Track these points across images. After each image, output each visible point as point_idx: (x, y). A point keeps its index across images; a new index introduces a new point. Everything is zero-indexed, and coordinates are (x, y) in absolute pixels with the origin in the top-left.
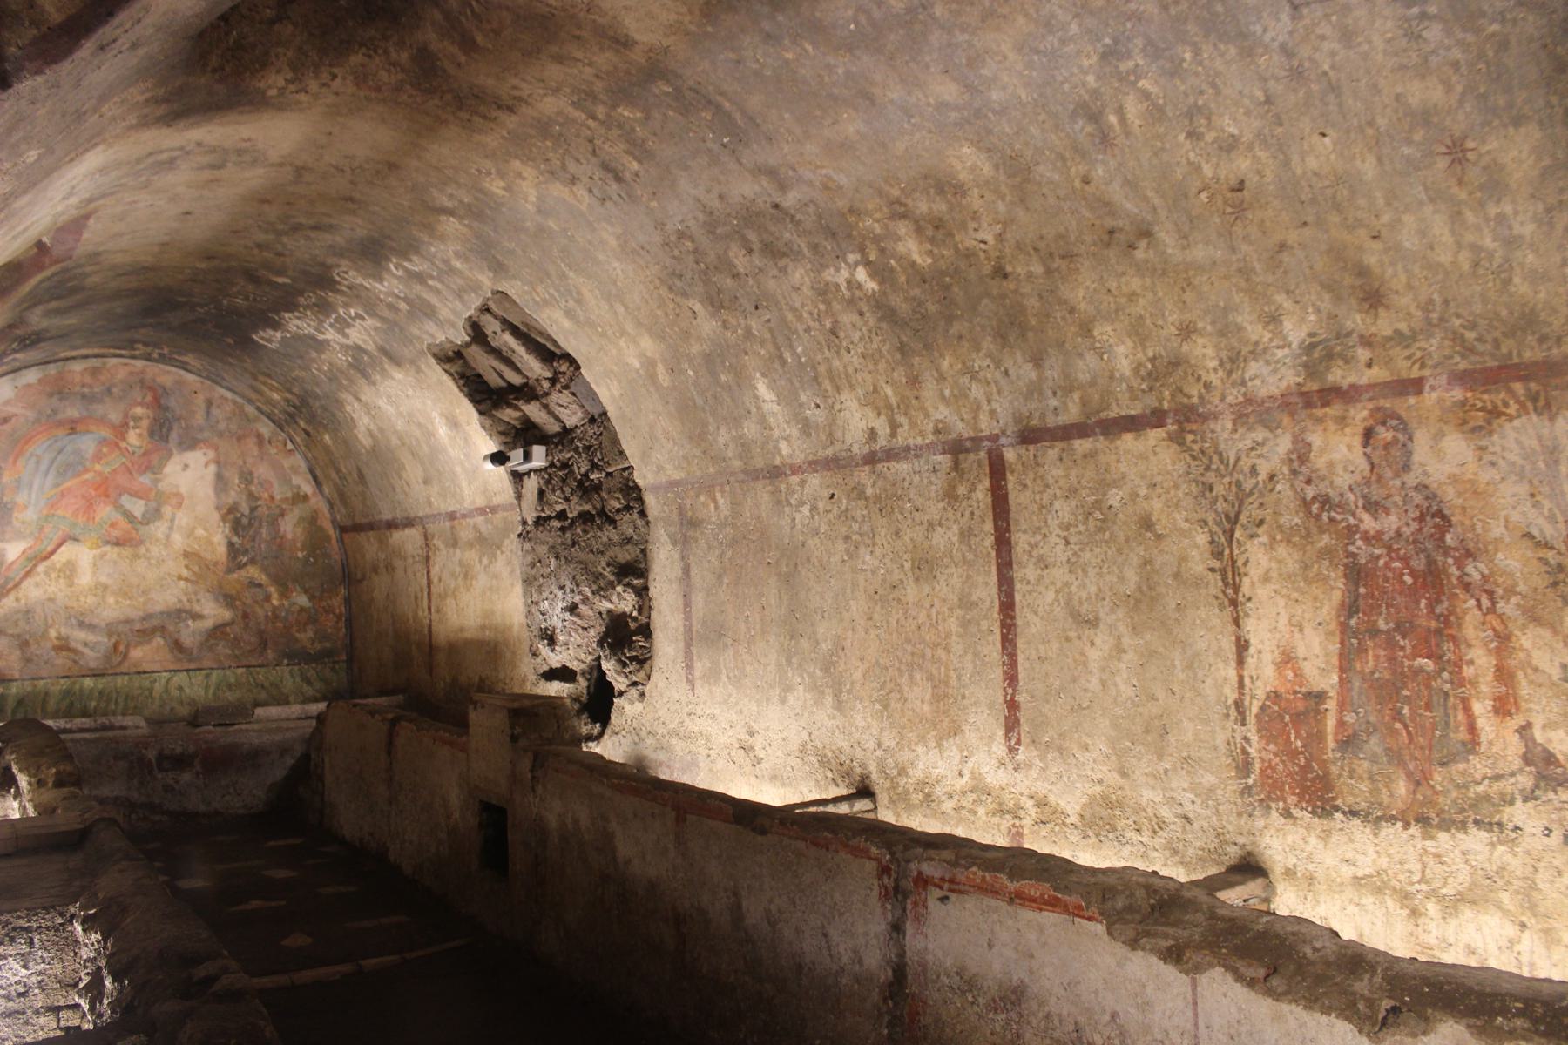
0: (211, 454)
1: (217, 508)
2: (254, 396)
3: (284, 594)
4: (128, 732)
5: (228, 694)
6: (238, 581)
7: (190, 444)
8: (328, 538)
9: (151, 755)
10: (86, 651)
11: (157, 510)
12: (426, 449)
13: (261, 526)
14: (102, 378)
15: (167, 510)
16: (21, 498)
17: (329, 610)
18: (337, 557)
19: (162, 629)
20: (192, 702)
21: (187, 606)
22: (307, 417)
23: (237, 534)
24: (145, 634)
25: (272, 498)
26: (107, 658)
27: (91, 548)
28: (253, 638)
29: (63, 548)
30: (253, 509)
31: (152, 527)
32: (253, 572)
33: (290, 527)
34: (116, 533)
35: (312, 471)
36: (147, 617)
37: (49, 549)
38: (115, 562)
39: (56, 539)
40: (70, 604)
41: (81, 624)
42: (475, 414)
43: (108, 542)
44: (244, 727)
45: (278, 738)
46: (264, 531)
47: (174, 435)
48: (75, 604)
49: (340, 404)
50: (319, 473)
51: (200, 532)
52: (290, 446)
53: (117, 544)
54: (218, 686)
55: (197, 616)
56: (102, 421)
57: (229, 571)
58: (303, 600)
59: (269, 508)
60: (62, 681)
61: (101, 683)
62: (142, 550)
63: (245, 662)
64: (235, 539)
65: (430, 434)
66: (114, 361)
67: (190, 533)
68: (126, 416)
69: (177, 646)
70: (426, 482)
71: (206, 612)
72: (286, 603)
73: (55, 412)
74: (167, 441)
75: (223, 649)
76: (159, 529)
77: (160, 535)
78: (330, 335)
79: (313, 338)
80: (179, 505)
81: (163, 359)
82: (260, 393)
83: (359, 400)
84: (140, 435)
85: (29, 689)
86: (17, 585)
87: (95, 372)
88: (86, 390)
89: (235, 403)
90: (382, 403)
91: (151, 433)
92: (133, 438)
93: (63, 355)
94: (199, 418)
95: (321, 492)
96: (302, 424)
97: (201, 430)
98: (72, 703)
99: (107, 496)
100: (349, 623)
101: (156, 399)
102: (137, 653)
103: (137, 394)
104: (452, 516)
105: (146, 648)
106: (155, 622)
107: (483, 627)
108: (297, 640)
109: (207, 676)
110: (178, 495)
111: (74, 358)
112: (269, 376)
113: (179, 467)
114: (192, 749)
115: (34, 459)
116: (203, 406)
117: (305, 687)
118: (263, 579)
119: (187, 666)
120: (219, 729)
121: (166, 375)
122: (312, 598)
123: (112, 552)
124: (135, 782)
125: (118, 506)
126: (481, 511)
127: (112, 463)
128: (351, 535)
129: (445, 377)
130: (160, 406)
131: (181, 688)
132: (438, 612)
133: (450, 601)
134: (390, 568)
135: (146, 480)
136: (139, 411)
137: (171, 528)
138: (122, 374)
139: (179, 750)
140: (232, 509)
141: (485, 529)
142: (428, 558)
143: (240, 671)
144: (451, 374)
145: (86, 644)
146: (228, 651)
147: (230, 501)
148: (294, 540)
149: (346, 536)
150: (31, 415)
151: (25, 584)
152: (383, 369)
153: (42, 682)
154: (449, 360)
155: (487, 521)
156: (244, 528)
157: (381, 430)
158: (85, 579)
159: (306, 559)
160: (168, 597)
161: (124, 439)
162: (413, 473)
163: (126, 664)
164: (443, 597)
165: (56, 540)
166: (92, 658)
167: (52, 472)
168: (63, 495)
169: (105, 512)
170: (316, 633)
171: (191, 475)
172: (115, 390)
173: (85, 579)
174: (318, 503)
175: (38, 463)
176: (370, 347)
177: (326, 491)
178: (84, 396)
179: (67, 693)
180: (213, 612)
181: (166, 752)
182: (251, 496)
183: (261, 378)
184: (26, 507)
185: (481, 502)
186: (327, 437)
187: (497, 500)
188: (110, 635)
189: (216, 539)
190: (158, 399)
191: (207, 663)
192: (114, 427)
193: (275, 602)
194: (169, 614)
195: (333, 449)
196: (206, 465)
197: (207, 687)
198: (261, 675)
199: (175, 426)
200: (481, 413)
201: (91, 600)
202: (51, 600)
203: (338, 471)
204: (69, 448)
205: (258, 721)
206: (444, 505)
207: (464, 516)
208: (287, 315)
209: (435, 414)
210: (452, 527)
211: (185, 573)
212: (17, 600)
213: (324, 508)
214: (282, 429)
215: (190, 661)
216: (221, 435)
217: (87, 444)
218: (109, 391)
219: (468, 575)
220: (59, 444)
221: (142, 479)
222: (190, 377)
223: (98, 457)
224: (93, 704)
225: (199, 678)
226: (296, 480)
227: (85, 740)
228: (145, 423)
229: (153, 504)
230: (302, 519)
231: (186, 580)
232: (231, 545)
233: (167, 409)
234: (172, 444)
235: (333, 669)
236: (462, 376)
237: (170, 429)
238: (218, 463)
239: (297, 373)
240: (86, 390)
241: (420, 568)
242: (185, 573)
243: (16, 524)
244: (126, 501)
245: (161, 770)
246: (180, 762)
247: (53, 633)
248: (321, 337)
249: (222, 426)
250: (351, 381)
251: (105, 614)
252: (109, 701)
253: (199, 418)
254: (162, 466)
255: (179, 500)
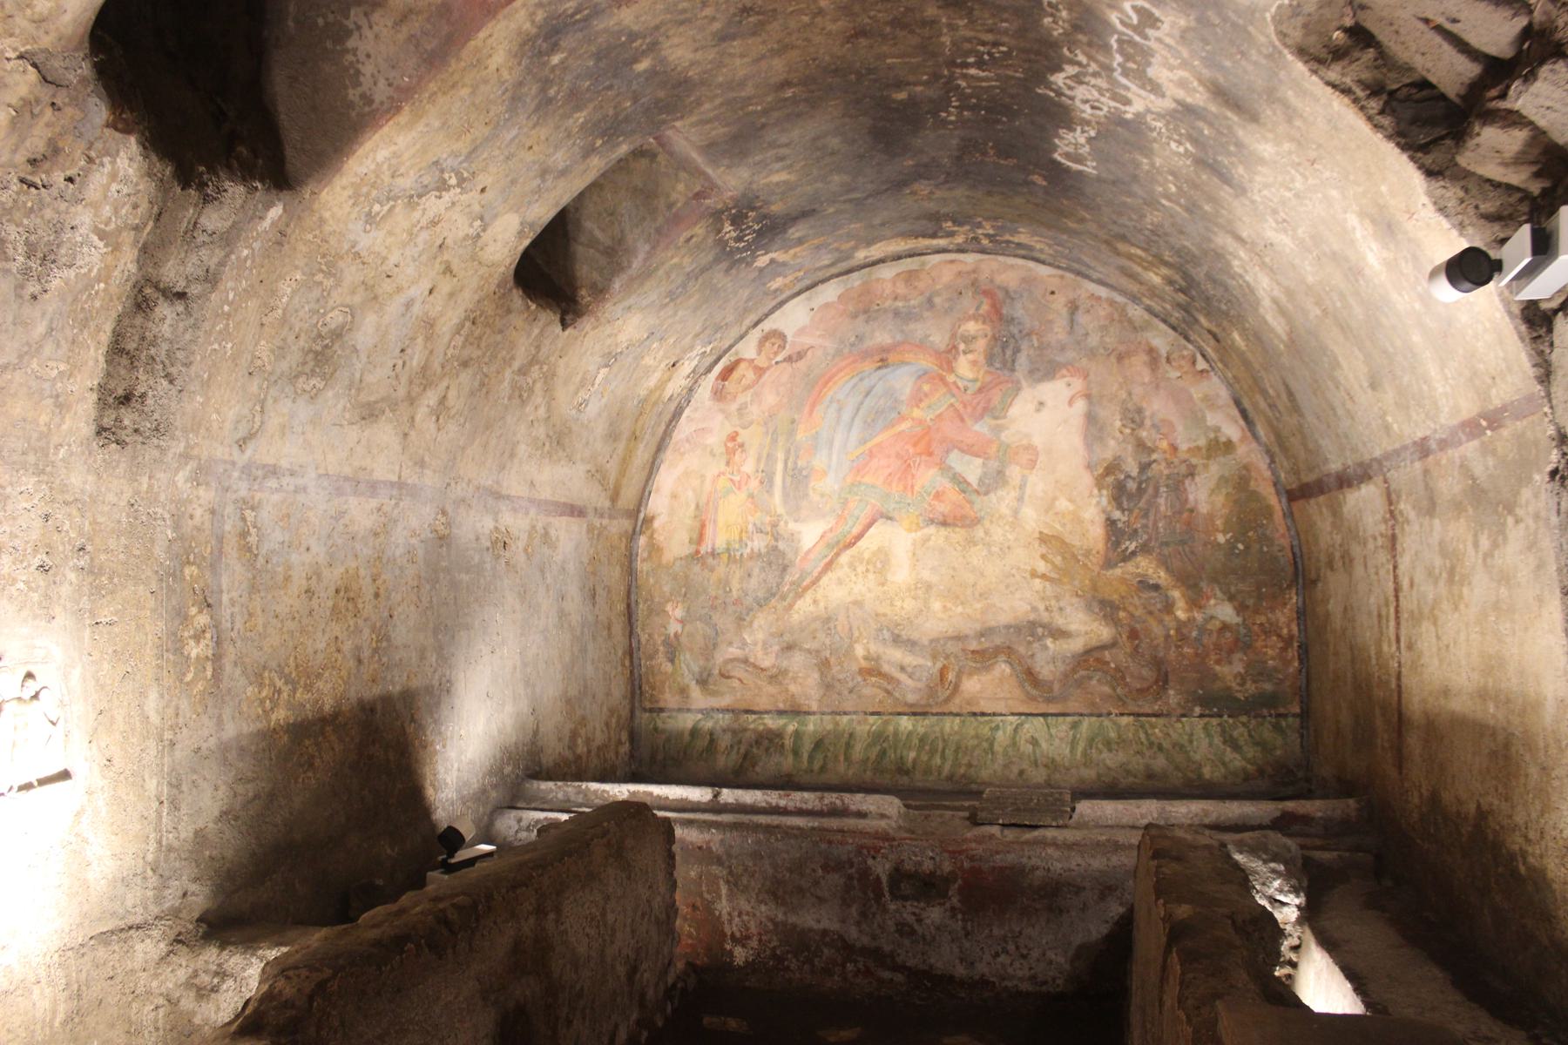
0: (1078, 384)
1: (1089, 467)
2: (1134, 287)
3: (1195, 603)
4: (861, 824)
5: (1105, 755)
6: (1123, 580)
7: (1046, 370)
8: (1268, 512)
9: (881, 868)
10: (903, 677)
11: (1000, 473)
12: (1358, 311)
13: (1156, 494)
14: (921, 285)
15: (1014, 472)
16: (819, 461)
17: (1269, 630)
18: (1285, 542)
19: (1008, 651)
20: (1052, 765)
21: (1045, 617)
22: (1198, 304)
23: (1120, 507)
24: (983, 658)
25: (1174, 448)
26: (931, 691)
27: (910, 530)
28: (1141, 669)
29: (872, 530)
30: (1144, 467)
31: (992, 495)
32: (1145, 566)
33: (1205, 495)
34: (942, 508)
35: (1238, 403)
36: (984, 633)
37: (855, 531)
38: (942, 551)
39: (864, 515)
40: (881, 610)
41: (897, 640)
42: (1416, 178)
43: (932, 521)
44: (1050, 833)
45: (1097, 863)
46: (1161, 501)
47: (1022, 360)
48: (888, 610)
49: (1219, 255)
50: (1246, 404)
51: (1063, 504)
52: (1201, 364)
53: (944, 524)
54: (1091, 742)
55: (1060, 634)
56: (922, 345)
57: (1108, 564)
58: (1226, 612)
59: (1169, 464)
60: (872, 719)
61: (923, 726)
62: (979, 533)
63: (1133, 708)
64: (1117, 514)
65: (1355, 272)
66: (937, 258)
67: (1049, 506)
68: (953, 336)
69: (1030, 676)
70: (1374, 386)
71: (1073, 627)
72: (1199, 617)
73: (860, 338)
74: (1013, 370)
75: (1099, 687)
76: (1002, 501)
77: (1005, 510)
78: (1139, 102)
79: (1123, 123)
80: (1032, 464)
81: (998, 247)
82: (1132, 276)
83: (1239, 239)
84: (974, 363)
85: (830, 727)
86: (815, 582)
87: (910, 276)
88: (900, 304)
89: (1112, 303)
90: (1270, 232)
91: (990, 358)
92: (966, 368)
93: (861, 255)
94: (1059, 332)
95: (1255, 436)
96: (1202, 320)
97: (1063, 349)
98: (883, 753)
99: (930, 454)
100: (1304, 651)
101: (996, 309)
102: (971, 685)
103: (968, 303)
104: (1423, 449)
105: (986, 678)
106: (998, 641)
107: (1483, 695)
108: (1215, 677)
109: (1075, 726)
110: (1030, 448)
111: (882, 261)
112: (1123, 238)
113: (1031, 407)
114: (947, 867)
115: (835, 405)
116: (1064, 312)
117: (1229, 754)
118: (1162, 577)
119: (1043, 708)
120: (1010, 834)
121: (1006, 271)
122: (1241, 609)
123: (937, 535)
124: (854, 911)
125: (945, 468)
126: (1471, 428)
127: (941, 402)
128: (1301, 503)
129: (1339, 106)
130: (1001, 317)
131: (1034, 742)
132: (1410, 647)
133: (1426, 626)
134: (1348, 560)
135: (982, 428)
136: (972, 327)
137: (1020, 499)
138: (947, 276)
139: (928, 866)
140: (1111, 469)
141: (1481, 467)
142: (1394, 538)
143: (1125, 720)
144: (1346, 91)
145: (902, 669)
146: (1106, 689)
147: (1109, 455)
148: (1211, 517)
149: (1296, 506)
150: (831, 345)
151: (825, 580)
152: (1239, 145)
153: (845, 719)
154: (1338, 54)
155: (1486, 450)
156: (1130, 497)
157: (1289, 293)
158: (901, 575)
159: (1231, 545)
160: (1018, 603)
161: (951, 370)
162: (1352, 369)
163: (957, 700)
164: (1417, 618)
165: (864, 521)
166: (911, 690)
167: (858, 422)
168: (871, 454)
169: (928, 477)
170: (1248, 665)
171: (1049, 421)
172: (937, 300)
173: (901, 575)
174: (1249, 453)
175: (840, 410)
176: (1199, 98)
177: (1261, 431)
178: (897, 313)
179: (878, 737)
180: (1084, 627)
181: (908, 866)
182: (1141, 446)
183: (1121, 246)
184: (825, 473)
185: (1468, 408)
186: (1236, 336)
187: (1502, 394)
188: (934, 657)
189: (1087, 514)
190: (997, 306)
191: (1073, 706)
192: (938, 354)
193: (1181, 614)
194: (1018, 629)
195: (1249, 355)
196: (1071, 402)
197: (1073, 743)
198: (1158, 729)
199: (1024, 345)
200: (1430, 173)
201: (909, 605)
202: (858, 603)
203: (1264, 392)
204: (879, 389)
205: (1080, 826)
206: (1411, 428)
207: (1444, 444)
208: (1059, 79)
209: (1352, 220)
210: (1426, 472)
211: (1042, 567)
212: (815, 602)
213: (1261, 463)
214: (1187, 338)
215: (1049, 701)
216: (1092, 354)
217: (902, 380)
218: (930, 301)
219: (1454, 575)
220: (866, 383)
221: (977, 427)
222: (1043, 270)
223: (918, 399)
224: (912, 755)
225: (1062, 727)
226: (1212, 419)
227: (788, 832)
228: (981, 344)
229: (994, 464)
230: (1223, 480)
231: (1043, 576)
232: (1111, 523)
233: (1011, 320)
234: (1019, 374)
235: (1276, 727)
236: (1375, 90)
237: (1017, 350)
238: (1088, 397)
239: (1152, 218)
240: (900, 304)
241: (1383, 557)
242: (1042, 567)
243: (815, 498)
244: (956, 460)
245: (894, 897)
246: (928, 886)
247: (859, 651)
248: (1130, 112)
249: (1093, 340)
250: (1212, 199)
251: (928, 625)
252: (932, 752)
253: (1059, 332)
254: (1006, 407)
255: (1030, 454)
